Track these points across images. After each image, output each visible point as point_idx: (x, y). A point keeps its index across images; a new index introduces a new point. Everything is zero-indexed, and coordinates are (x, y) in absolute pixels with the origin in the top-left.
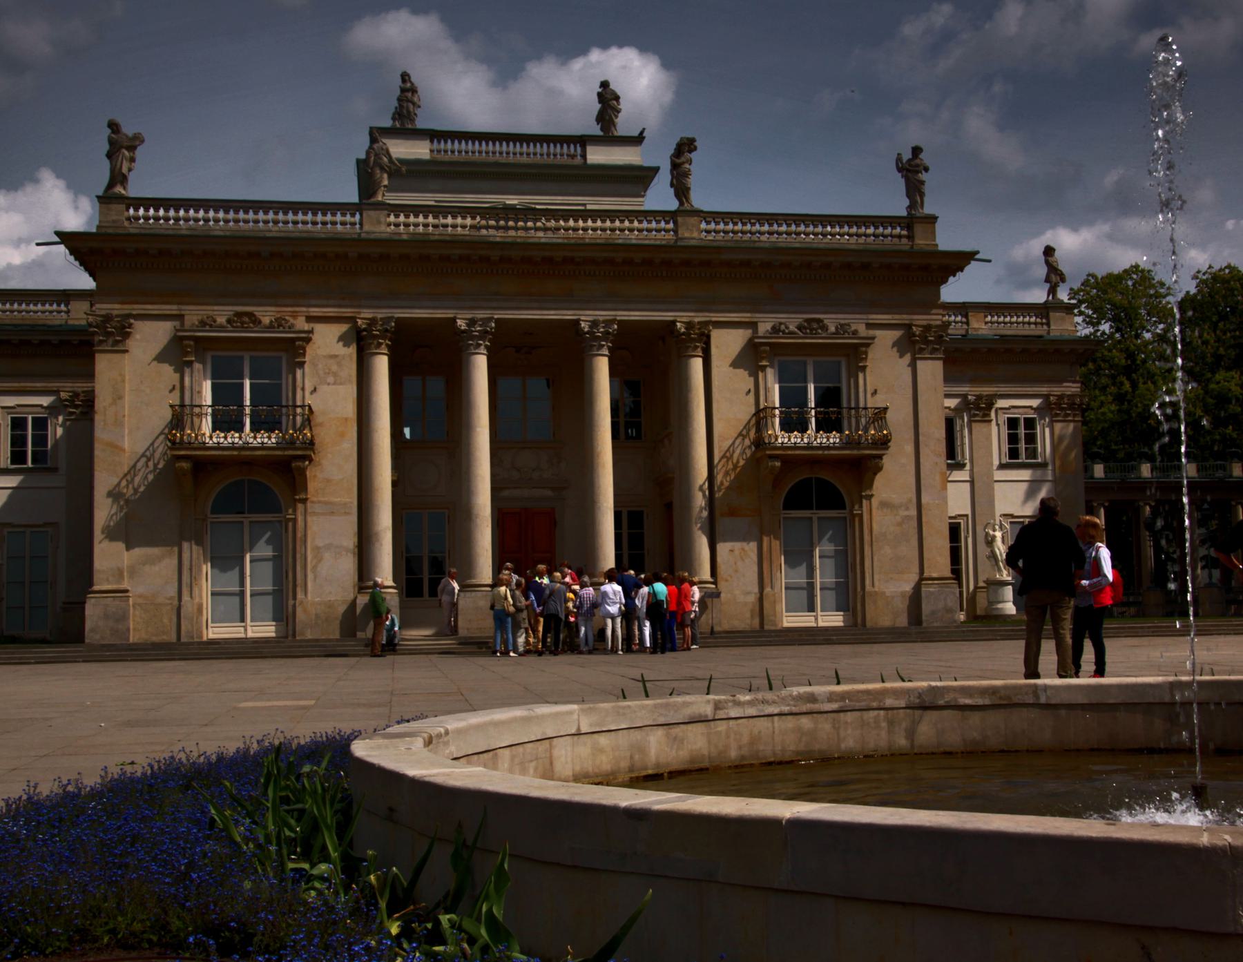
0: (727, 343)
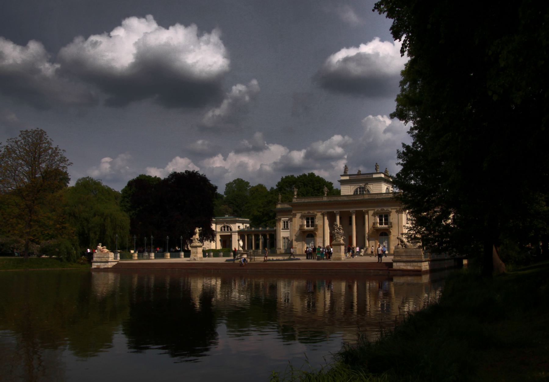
0: (371, 213)
